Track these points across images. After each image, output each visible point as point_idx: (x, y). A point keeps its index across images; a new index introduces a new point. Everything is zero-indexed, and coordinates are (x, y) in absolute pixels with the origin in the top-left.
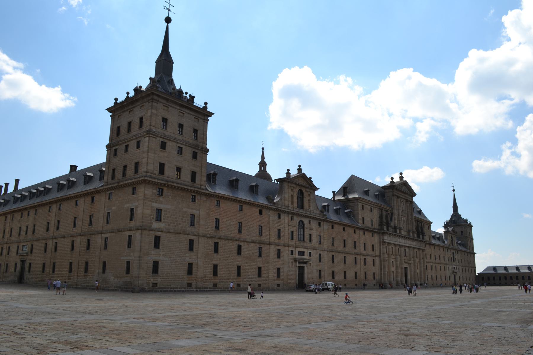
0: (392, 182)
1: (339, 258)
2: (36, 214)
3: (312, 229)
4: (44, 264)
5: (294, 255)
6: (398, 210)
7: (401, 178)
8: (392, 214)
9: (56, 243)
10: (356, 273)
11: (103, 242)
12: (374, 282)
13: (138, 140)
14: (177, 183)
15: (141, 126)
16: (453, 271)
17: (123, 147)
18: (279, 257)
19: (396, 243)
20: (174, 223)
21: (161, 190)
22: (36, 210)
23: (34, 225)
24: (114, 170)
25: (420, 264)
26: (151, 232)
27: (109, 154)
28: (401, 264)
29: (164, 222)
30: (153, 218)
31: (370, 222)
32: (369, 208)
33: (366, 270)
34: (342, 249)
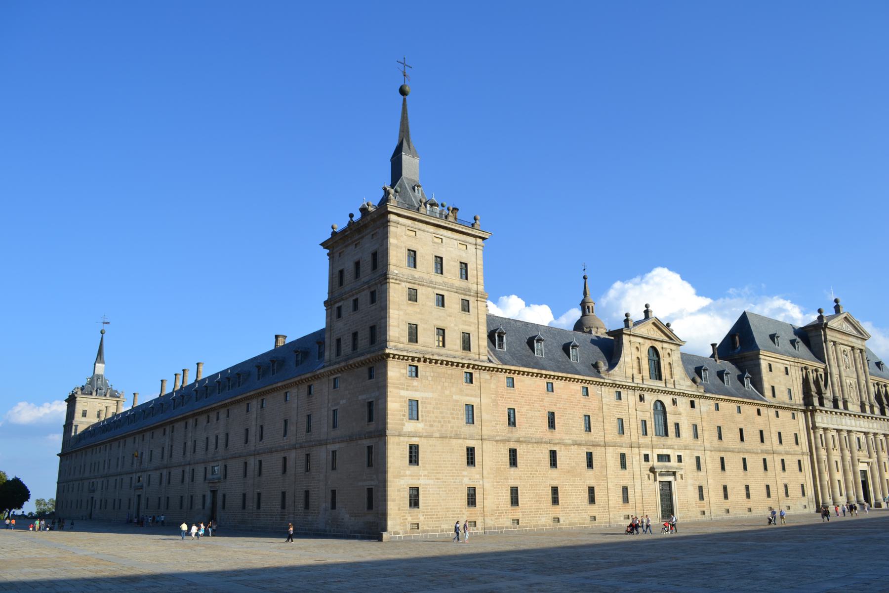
0: (820, 318)
1: (733, 463)
2: (228, 416)
3: (680, 414)
4: (244, 495)
5: (650, 464)
7: (837, 309)
9: (260, 462)
10: (768, 487)
11: (330, 457)
13: (373, 290)
14: (438, 355)
15: (375, 266)
17: (350, 303)
18: (623, 466)
19: (840, 427)
20: (440, 422)
21: (414, 369)
22: (228, 411)
23: (227, 435)
24: (339, 341)
26: (402, 439)
27: (329, 316)
28: (853, 465)
29: (422, 421)
30: (404, 415)
31: (786, 394)
33: (786, 481)
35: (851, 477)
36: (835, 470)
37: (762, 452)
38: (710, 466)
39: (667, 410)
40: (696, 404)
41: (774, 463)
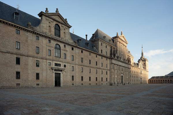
7: (122, 34)
8: (117, 50)
10: (97, 78)
12: (107, 82)
25: (128, 74)
28: (120, 74)
31: (105, 53)
32: (105, 45)
33: (102, 77)
34: (88, 65)
35: (119, 77)
36: (115, 75)
37: (96, 68)
38: (77, 70)
39: (61, 48)
41: (100, 71)
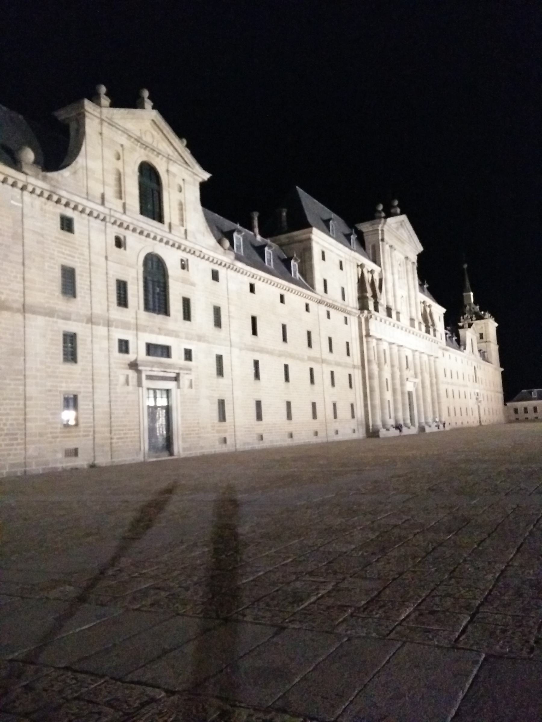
6: (393, 274)
8: (381, 280)
10: (314, 405)
12: (353, 424)
16: (477, 399)
28: (402, 385)
33: (334, 399)
35: (399, 397)
37: (310, 359)
40: (221, 276)
41: (322, 375)
